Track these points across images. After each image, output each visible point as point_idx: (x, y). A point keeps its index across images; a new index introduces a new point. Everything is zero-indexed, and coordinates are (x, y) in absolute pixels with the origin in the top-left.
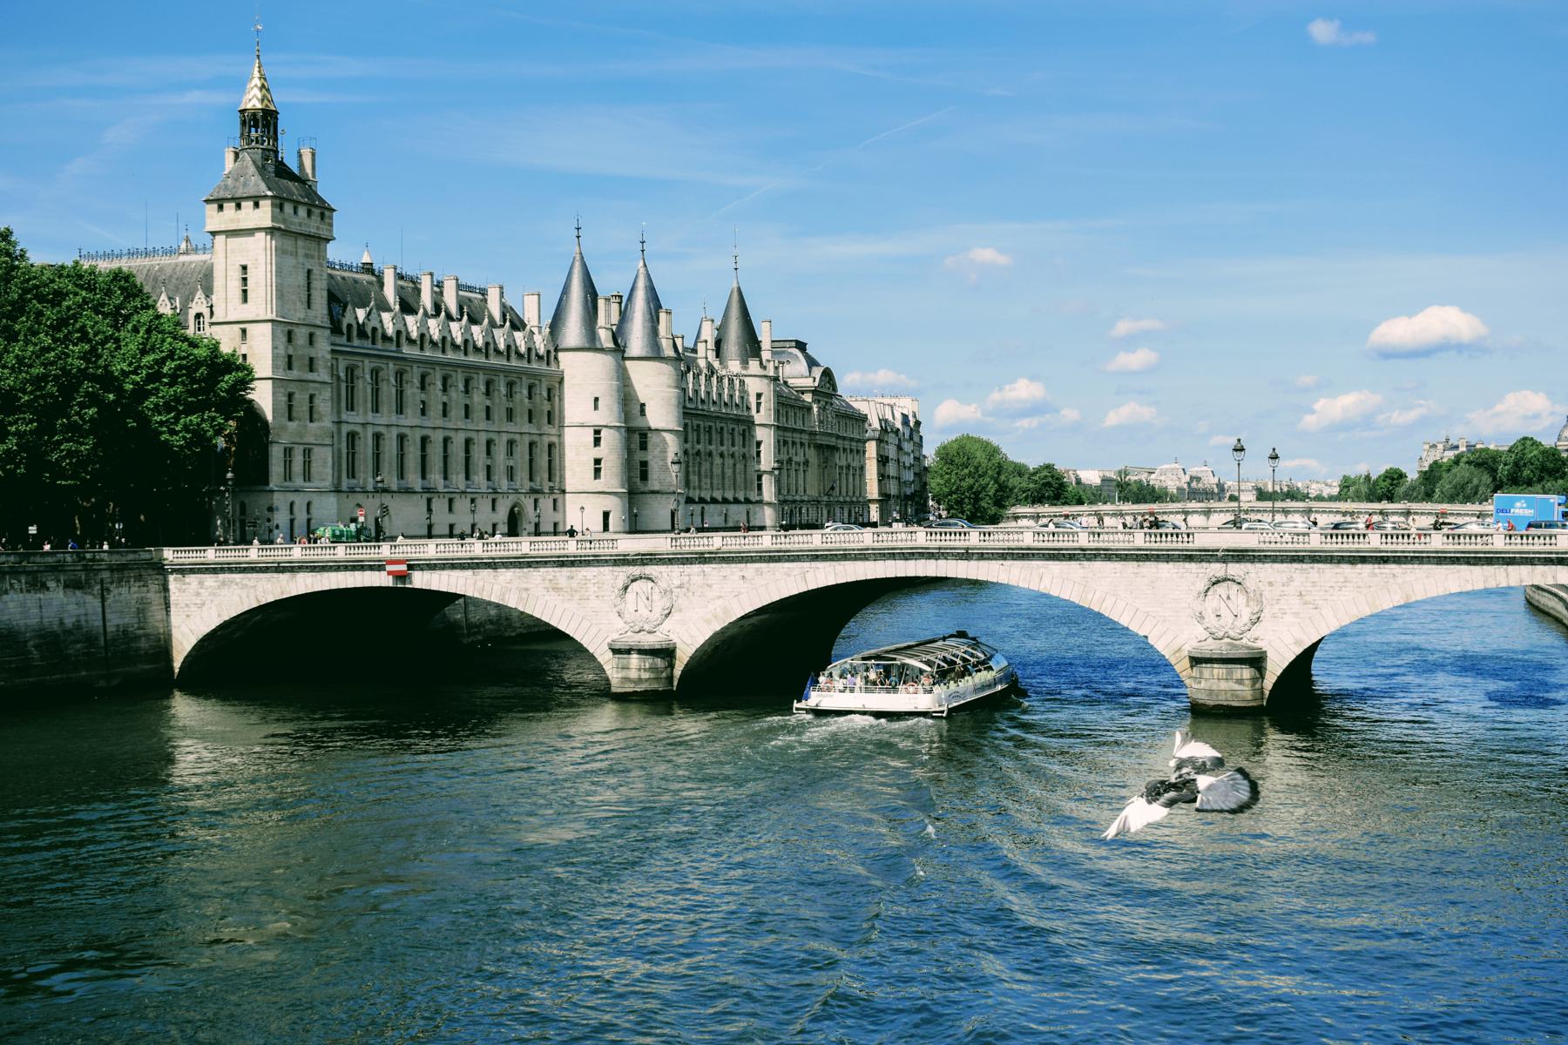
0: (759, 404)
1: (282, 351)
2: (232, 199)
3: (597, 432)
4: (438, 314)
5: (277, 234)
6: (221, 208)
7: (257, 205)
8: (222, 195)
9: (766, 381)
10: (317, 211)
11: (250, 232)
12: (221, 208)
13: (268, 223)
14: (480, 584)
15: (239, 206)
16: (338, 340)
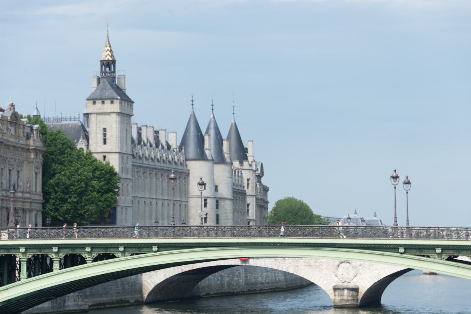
0: (248, 184)
1: (121, 166)
2: (101, 99)
3: (205, 200)
4: (157, 146)
5: (120, 114)
6: (94, 103)
7: (112, 102)
8: (95, 97)
9: (251, 172)
10: (129, 103)
11: (109, 113)
12: (94, 103)
13: (118, 110)
14: (278, 264)
15: (103, 103)
16: (135, 161)
